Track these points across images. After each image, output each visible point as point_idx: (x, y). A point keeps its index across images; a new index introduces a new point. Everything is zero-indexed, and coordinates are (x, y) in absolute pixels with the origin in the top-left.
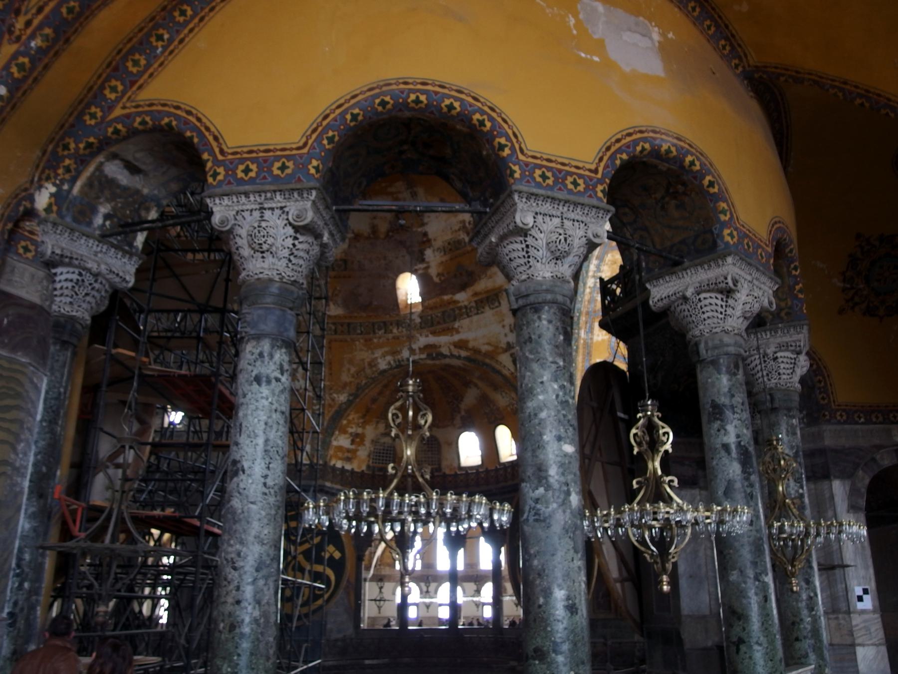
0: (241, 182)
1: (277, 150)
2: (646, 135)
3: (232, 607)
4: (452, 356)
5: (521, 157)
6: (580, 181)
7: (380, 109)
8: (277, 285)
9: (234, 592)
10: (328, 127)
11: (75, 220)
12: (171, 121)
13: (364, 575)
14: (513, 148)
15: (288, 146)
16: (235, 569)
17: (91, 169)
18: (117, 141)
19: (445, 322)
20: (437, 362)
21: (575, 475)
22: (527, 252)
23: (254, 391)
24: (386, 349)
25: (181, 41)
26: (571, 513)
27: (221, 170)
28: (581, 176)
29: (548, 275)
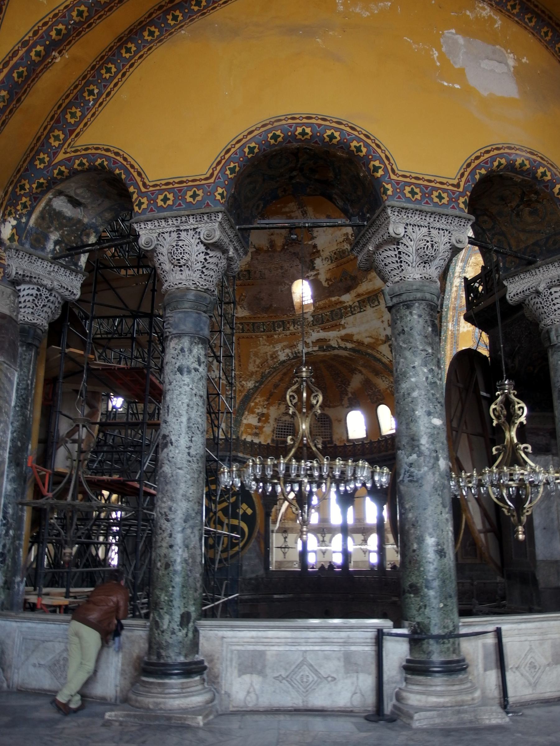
1: (189, 181)
2: (502, 151)
3: (166, 550)
4: (340, 348)
5: (393, 177)
6: (444, 195)
7: (272, 141)
8: (193, 292)
9: (167, 538)
10: (230, 160)
11: (32, 246)
12: (103, 161)
14: (385, 170)
15: (197, 178)
16: (168, 520)
17: (43, 204)
18: (62, 181)
19: (333, 320)
20: (328, 353)
21: (443, 443)
22: (400, 258)
23: (178, 379)
24: (285, 343)
25: (108, 94)
26: (440, 474)
27: (144, 200)
28: (445, 191)
29: (418, 276)
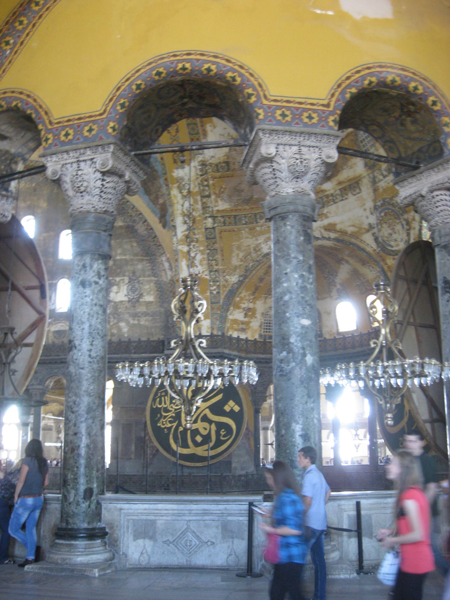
0: (63, 143)
2: (373, 70)
3: (72, 437)
4: (324, 238)
5: (265, 102)
6: (314, 115)
7: (157, 78)
8: (93, 215)
9: (73, 427)
10: (120, 97)
12: (17, 104)
13: (261, 424)
14: (258, 96)
15: (93, 114)
16: (73, 412)
21: (311, 341)
25: (22, 43)
26: (307, 369)
27: (50, 136)
28: (315, 111)
29: (290, 191)
